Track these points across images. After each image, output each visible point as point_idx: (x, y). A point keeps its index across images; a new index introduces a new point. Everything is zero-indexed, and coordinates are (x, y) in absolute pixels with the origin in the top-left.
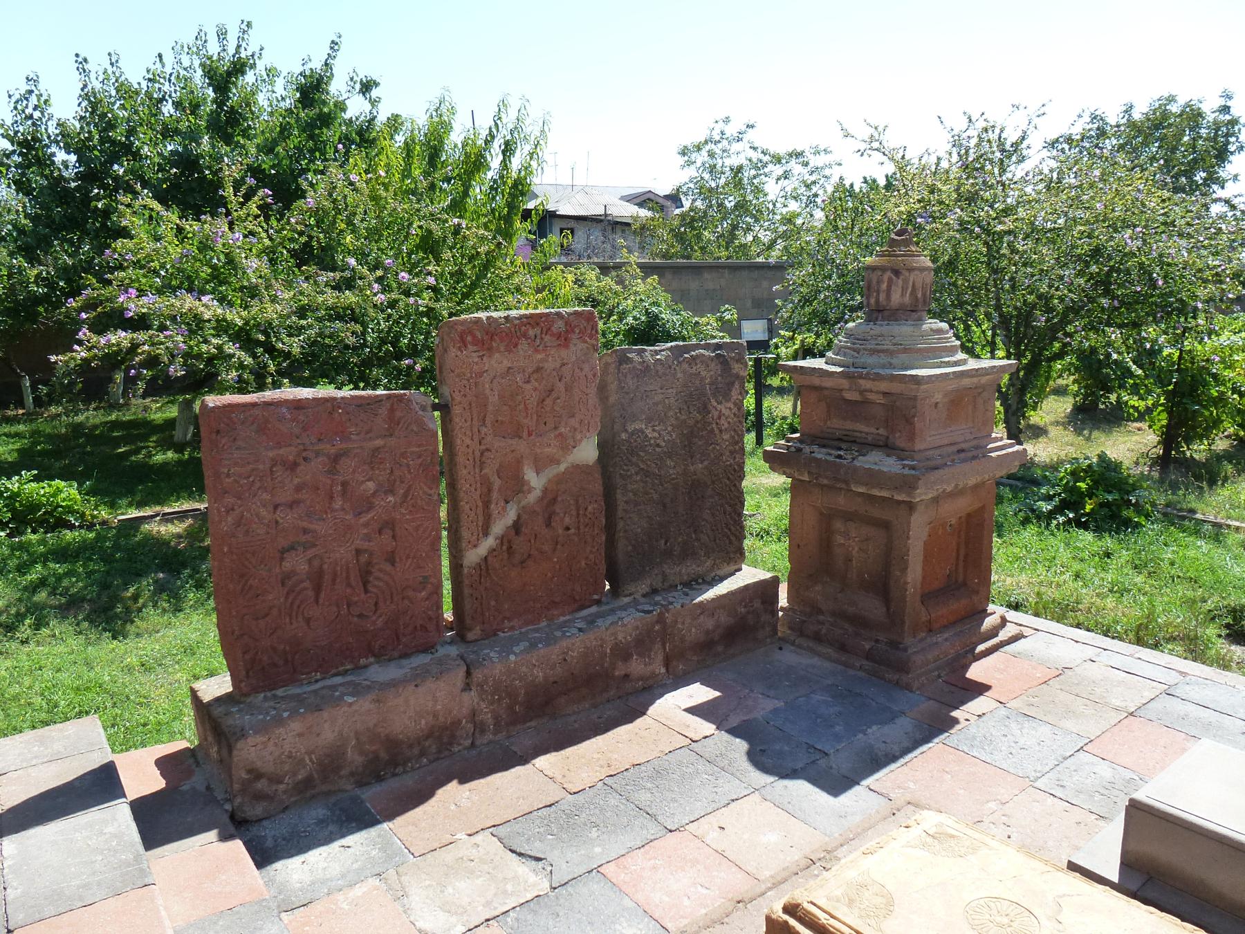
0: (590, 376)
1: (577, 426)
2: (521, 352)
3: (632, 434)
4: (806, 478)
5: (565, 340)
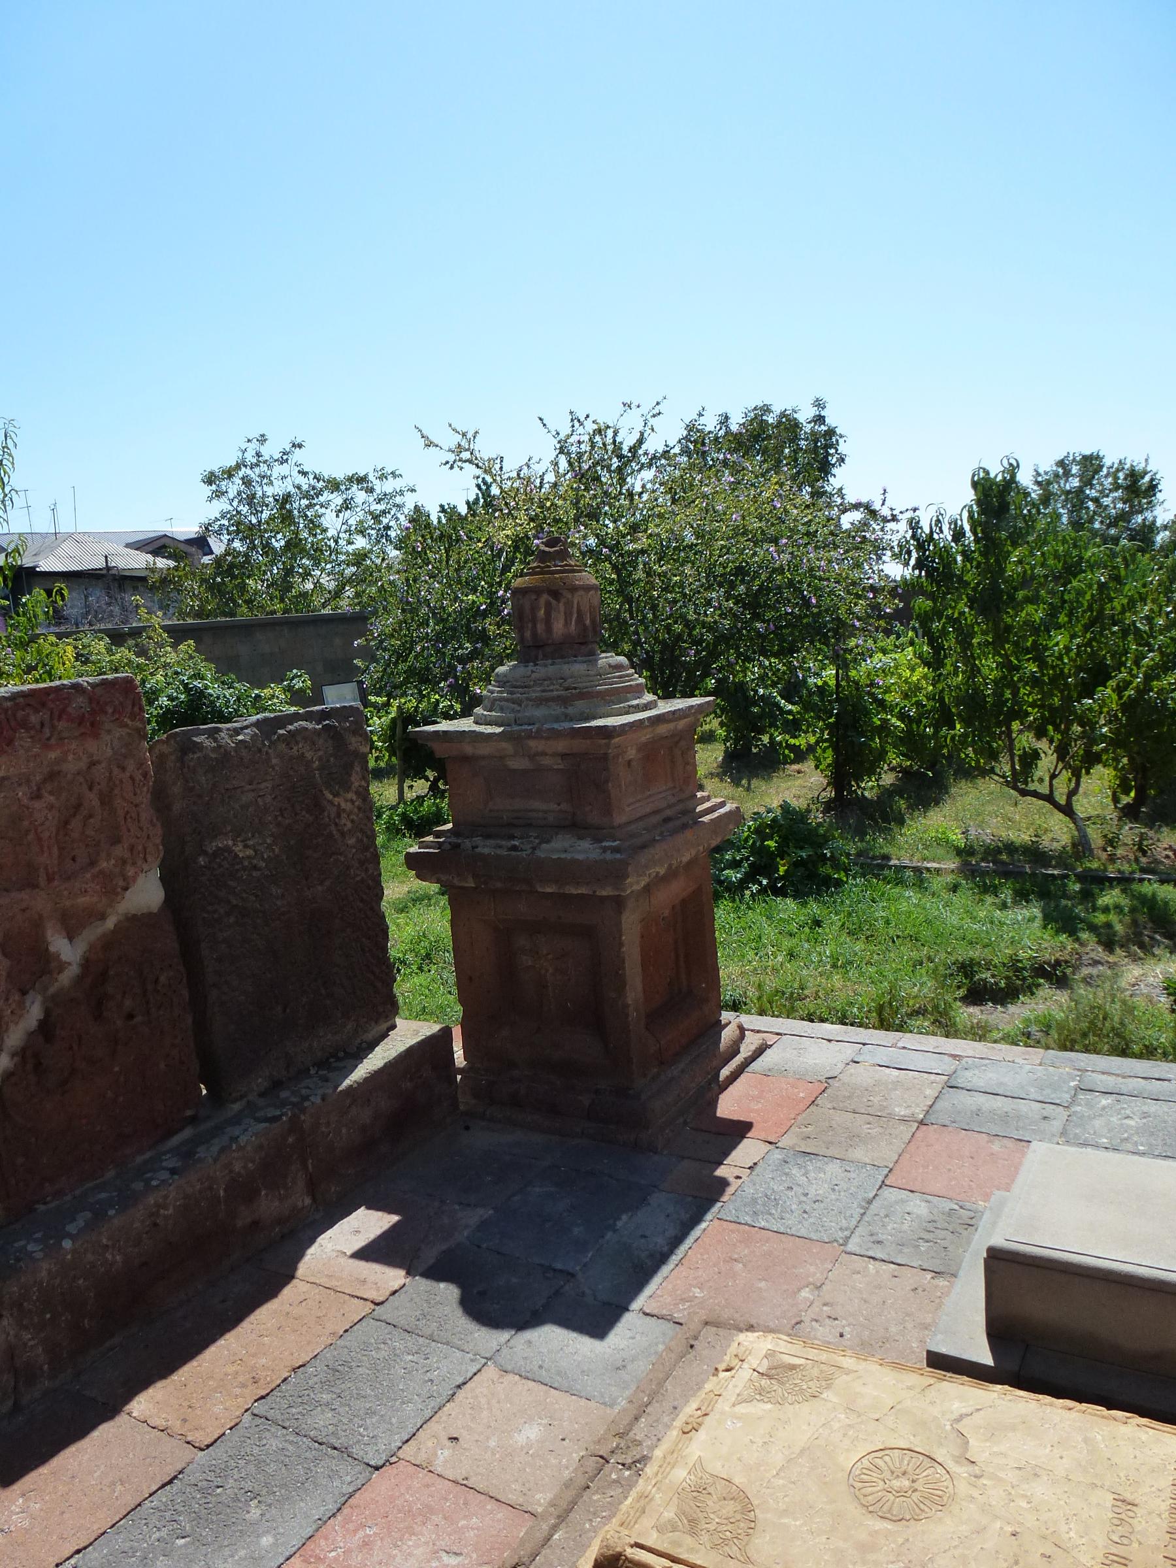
0: (138, 777)
1: (127, 855)
2: (22, 752)
3: (215, 854)
4: (471, 883)
5: (92, 724)
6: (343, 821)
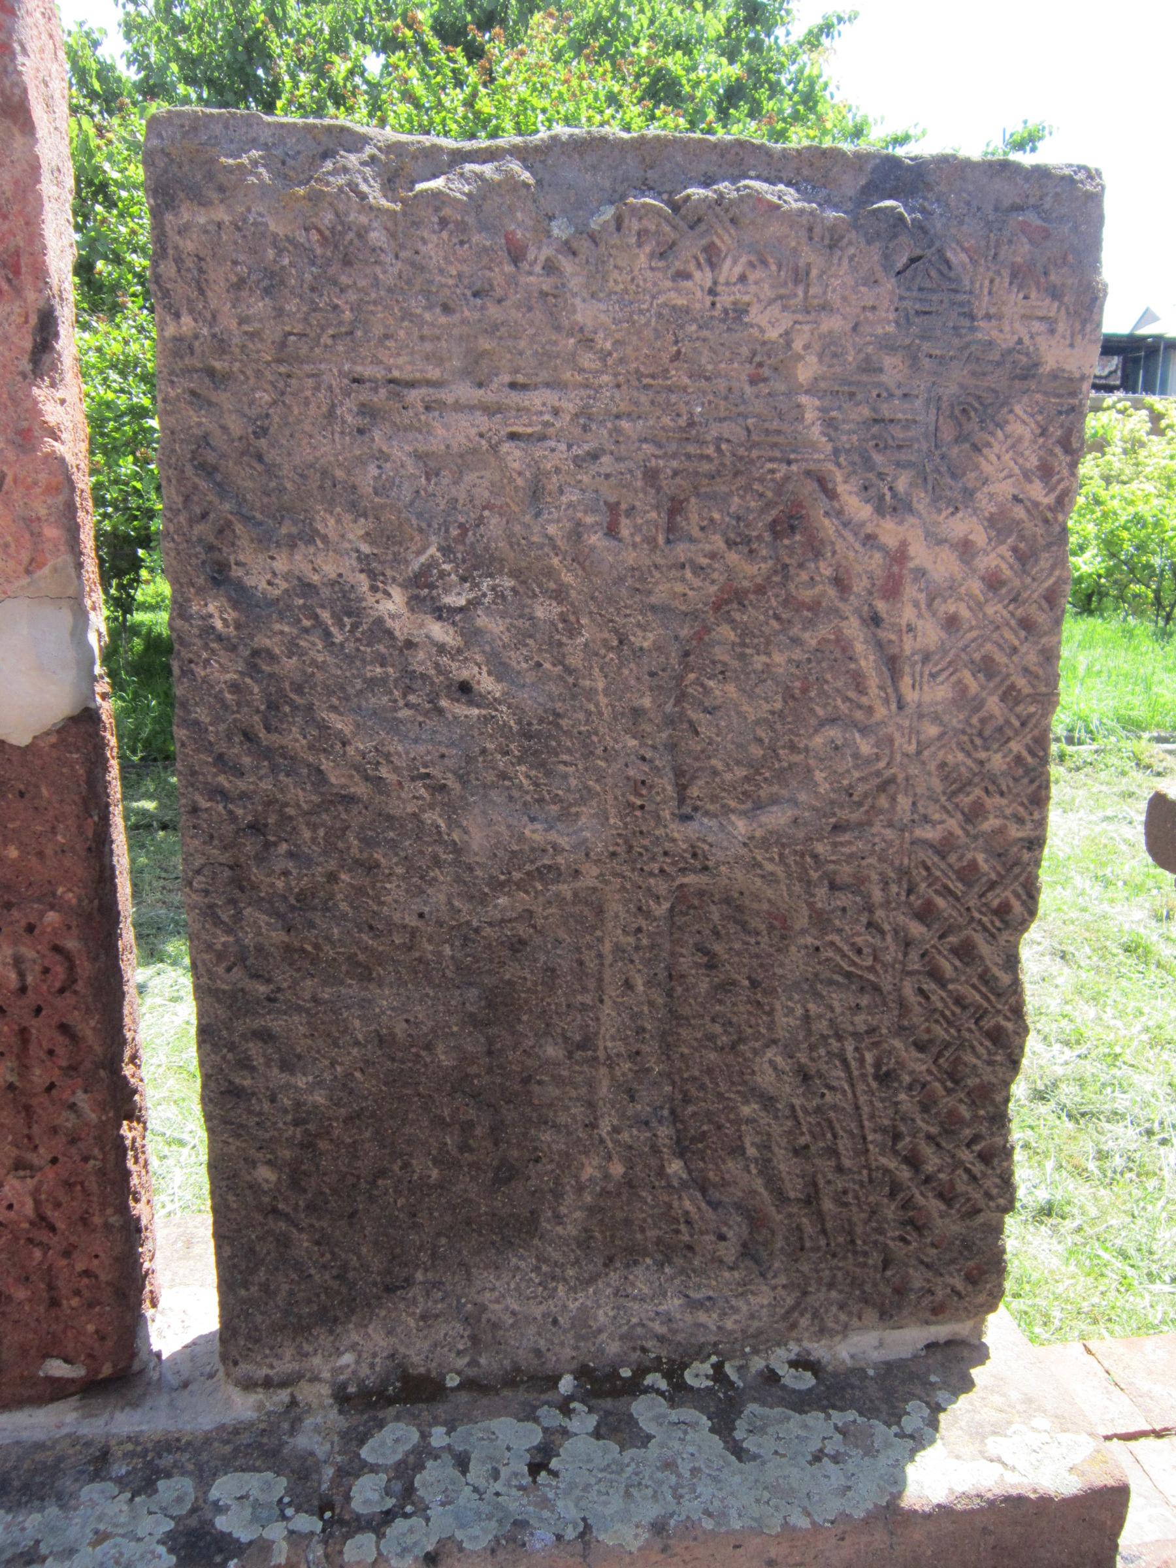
6: (908, 614)
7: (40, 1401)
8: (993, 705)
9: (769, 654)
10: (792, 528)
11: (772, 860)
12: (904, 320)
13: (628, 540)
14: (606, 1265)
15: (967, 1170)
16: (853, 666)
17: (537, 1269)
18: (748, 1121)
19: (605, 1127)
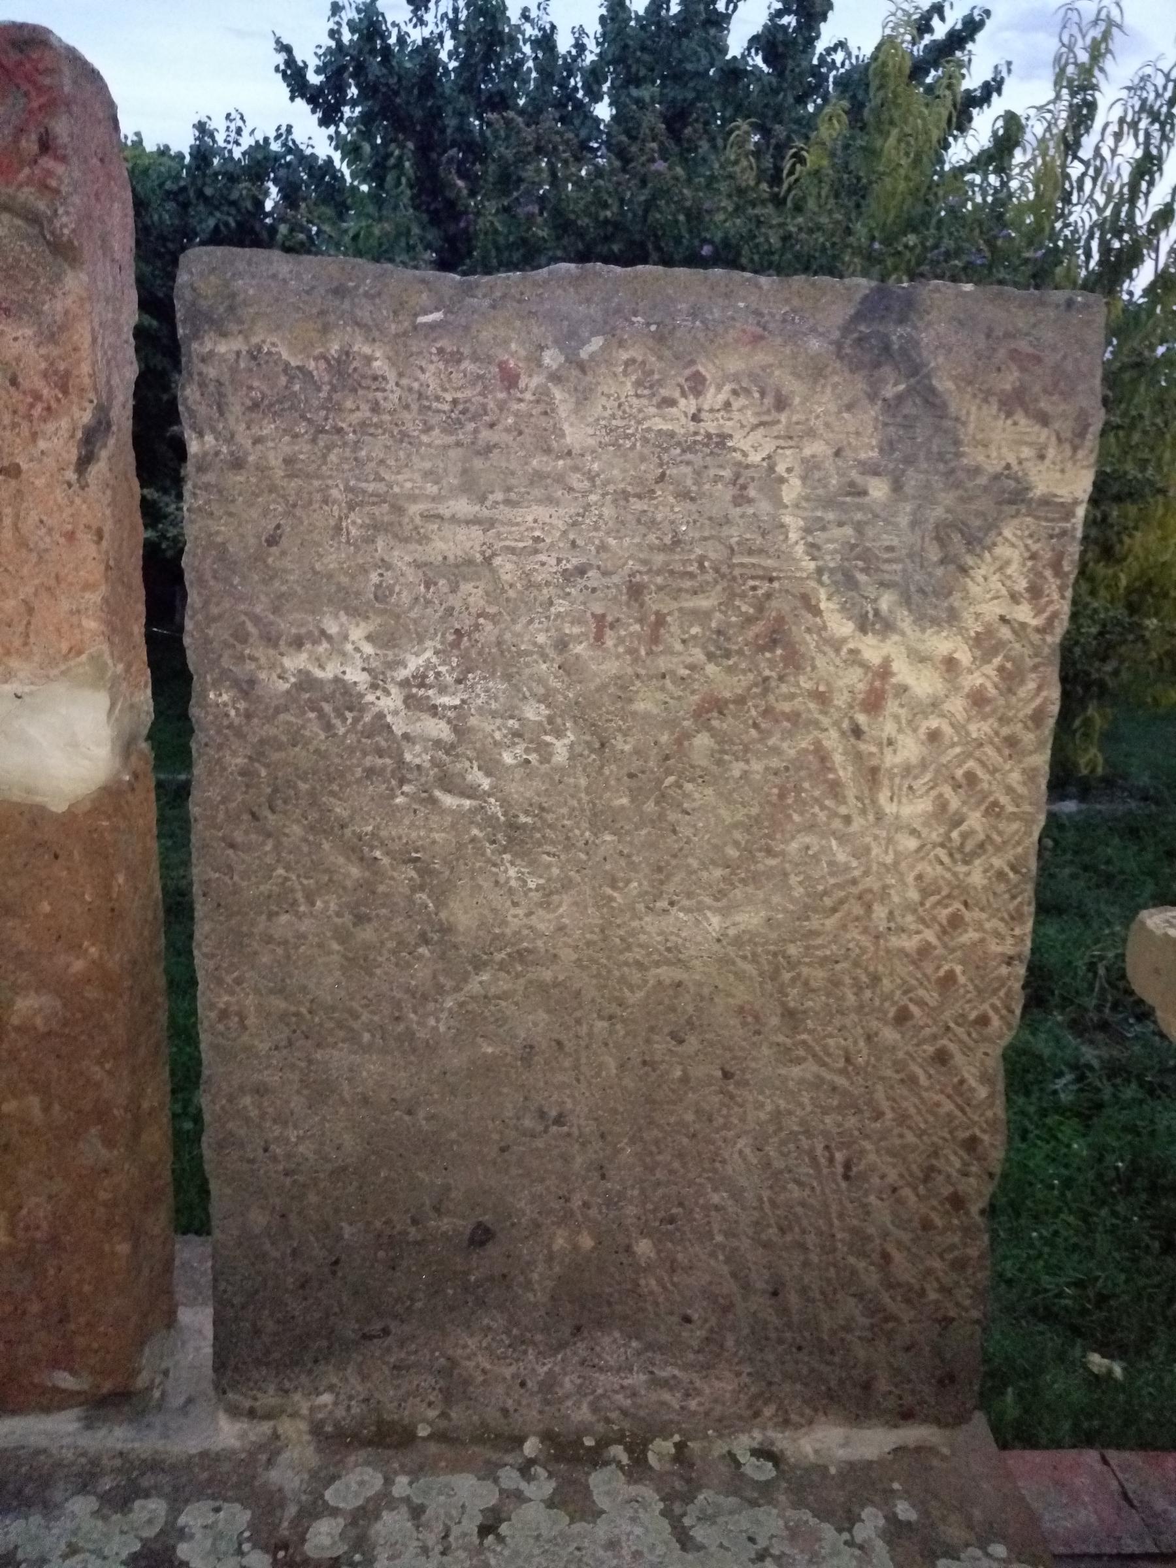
7: (47, 1410)
8: (975, 820)
9: (747, 762)
10: (775, 642)
11: (744, 958)
12: (887, 447)
13: (612, 650)
14: (574, 1335)
15: (937, 1279)
16: (831, 776)
17: (508, 1332)
18: (717, 1208)
19: (576, 1203)
